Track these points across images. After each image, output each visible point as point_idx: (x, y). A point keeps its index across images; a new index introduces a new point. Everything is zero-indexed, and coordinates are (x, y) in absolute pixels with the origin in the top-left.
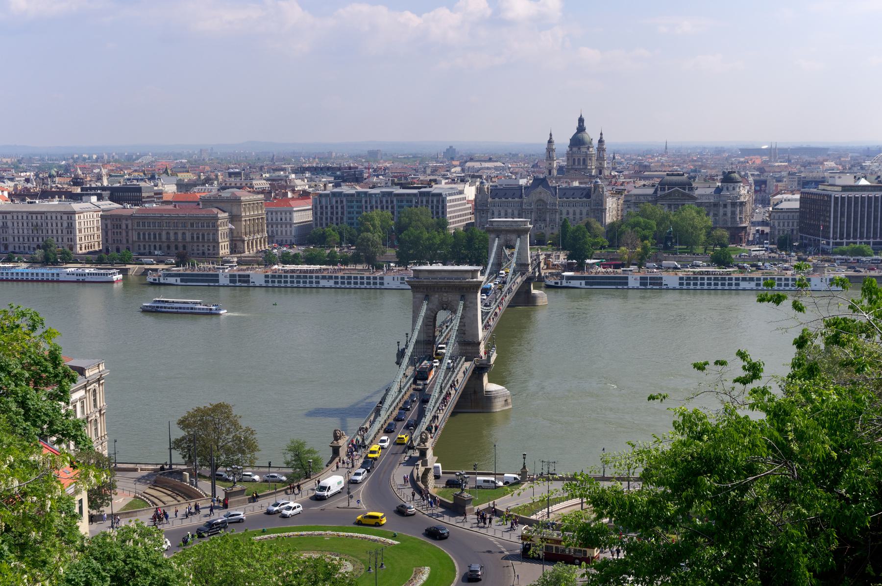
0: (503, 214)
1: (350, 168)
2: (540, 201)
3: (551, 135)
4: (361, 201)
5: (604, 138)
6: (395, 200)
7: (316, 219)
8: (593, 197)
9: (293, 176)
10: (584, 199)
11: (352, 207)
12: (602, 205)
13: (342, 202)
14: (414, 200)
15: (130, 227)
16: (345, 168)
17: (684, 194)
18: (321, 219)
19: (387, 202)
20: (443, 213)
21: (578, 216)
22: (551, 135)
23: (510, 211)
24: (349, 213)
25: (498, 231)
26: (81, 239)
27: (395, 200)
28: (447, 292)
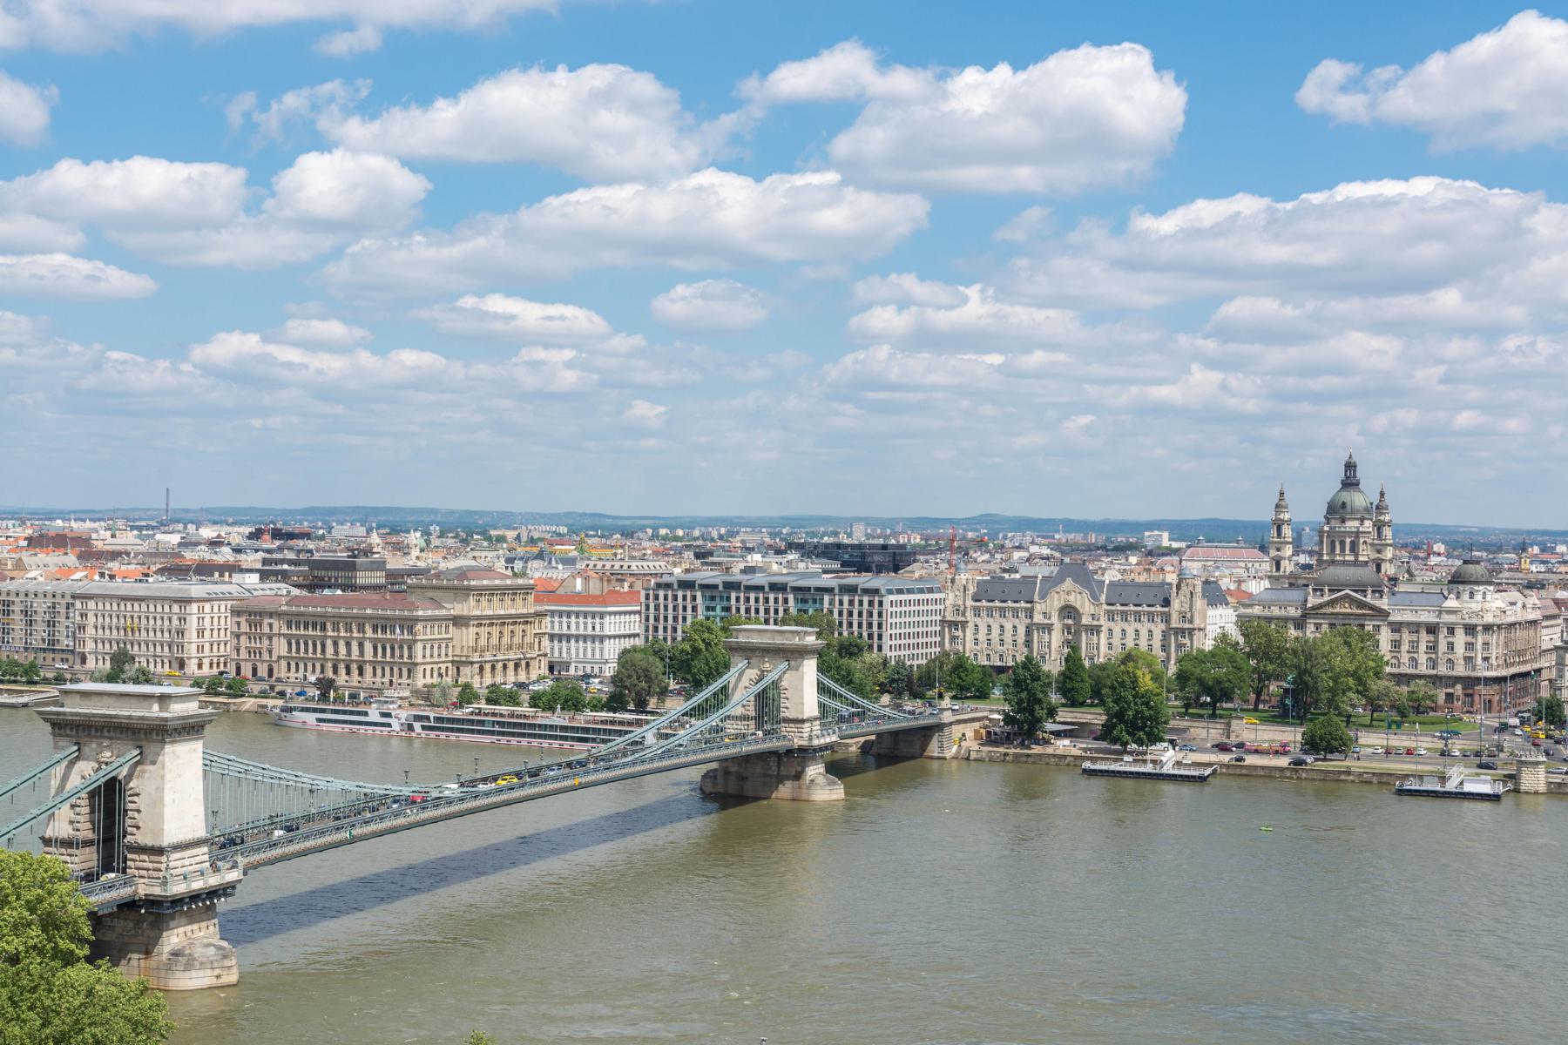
2: (1069, 611)
3: (1282, 494)
4: (728, 599)
5: (1388, 500)
6: (791, 597)
7: (647, 630)
8: (1175, 604)
11: (713, 609)
12: (1191, 622)
13: (694, 598)
14: (826, 598)
15: (275, 631)
17: (1361, 605)
19: (776, 600)
20: (880, 626)
22: (1282, 494)
23: (1008, 627)
25: (750, 652)
26: (200, 648)
27: (791, 597)
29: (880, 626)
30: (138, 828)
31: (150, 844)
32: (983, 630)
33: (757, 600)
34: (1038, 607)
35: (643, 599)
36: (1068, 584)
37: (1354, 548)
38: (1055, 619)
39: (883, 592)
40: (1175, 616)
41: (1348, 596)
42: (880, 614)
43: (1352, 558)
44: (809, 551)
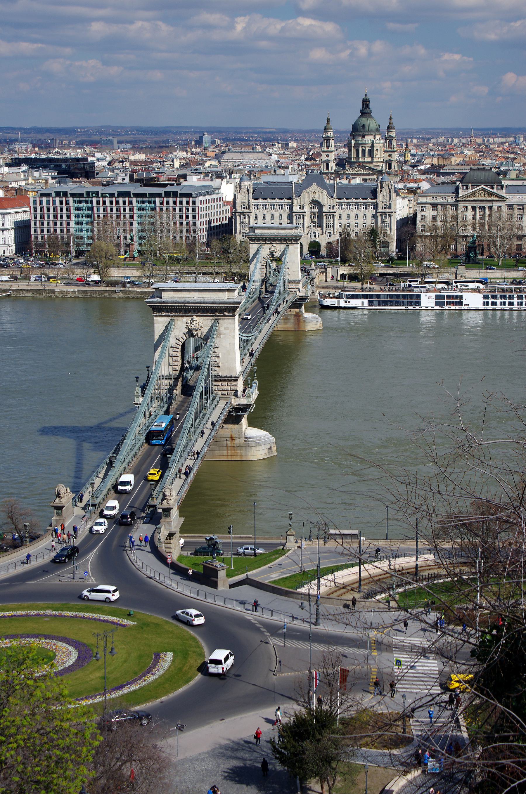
0: (268, 218)
1: (78, 160)
2: (316, 203)
3: (328, 120)
4: (92, 202)
5: (395, 123)
7: (35, 224)
8: (380, 196)
9: (6, 169)
10: (370, 200)
11: (81, 209)
12: (390, 207)
16: (73, 160)
17: (492, 194)
18: (42, 224)
19: (124, 203)
20: (194, 217)
21: (361, 222)
23: (277, 215)
24: (77, 216)
28: (197, 316)
29: (194, 217)
30: (219, 366)
31: (228, 376)
32: (260, 217)
33: (111, 203)
34: (296, 201)
35: (32, 204)
36: (314, 187)
37: (371, 153)
38: (307, 209)
39: (194, 195)
40: (380, 205)
41: (484, 190)
42: (194, 210)
43: (369, 160)
44: (34, 164)
